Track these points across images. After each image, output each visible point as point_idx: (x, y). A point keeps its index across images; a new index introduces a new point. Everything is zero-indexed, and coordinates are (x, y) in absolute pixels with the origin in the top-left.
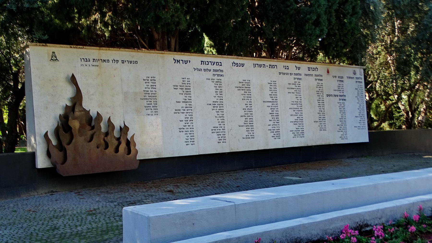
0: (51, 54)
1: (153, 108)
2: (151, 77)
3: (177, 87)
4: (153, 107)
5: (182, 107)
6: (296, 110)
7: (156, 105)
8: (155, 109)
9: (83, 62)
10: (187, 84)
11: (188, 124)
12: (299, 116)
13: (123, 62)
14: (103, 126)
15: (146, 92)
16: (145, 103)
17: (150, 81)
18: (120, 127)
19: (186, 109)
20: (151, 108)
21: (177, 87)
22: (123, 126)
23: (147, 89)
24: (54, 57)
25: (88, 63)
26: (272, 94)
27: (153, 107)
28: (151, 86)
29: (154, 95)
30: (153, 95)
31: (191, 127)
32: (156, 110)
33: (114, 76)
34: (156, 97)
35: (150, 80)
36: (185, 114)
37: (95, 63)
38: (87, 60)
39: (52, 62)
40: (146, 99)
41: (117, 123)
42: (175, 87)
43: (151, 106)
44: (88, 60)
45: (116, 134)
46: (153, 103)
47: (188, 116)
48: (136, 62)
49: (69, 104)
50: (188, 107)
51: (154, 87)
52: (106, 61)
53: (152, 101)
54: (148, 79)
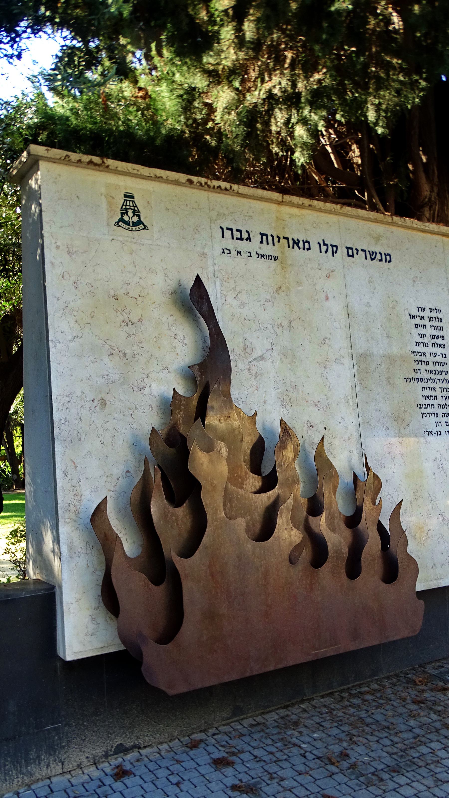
1: (440, 411)
4: (441, 406)
13: (351, 252)
15: (418, 357)
17: (426, 322)
18: (355, 477)
20: (436, 410)
23: (421, 349)
24: (130, 213)
25: (243, 245)
27: (441, 406)
28: (433, 337)
30: (438, 368)
33: (327, 298)
34: (446, 373)
35: (426, 318)
37: (267, 249)
38: (243, 236)
39: (122, 233)
44: (245, 235)
48: (387, 258)
51: (440, 341)
52: (301, 245)
53: (438, 386)
54: (422, 314)
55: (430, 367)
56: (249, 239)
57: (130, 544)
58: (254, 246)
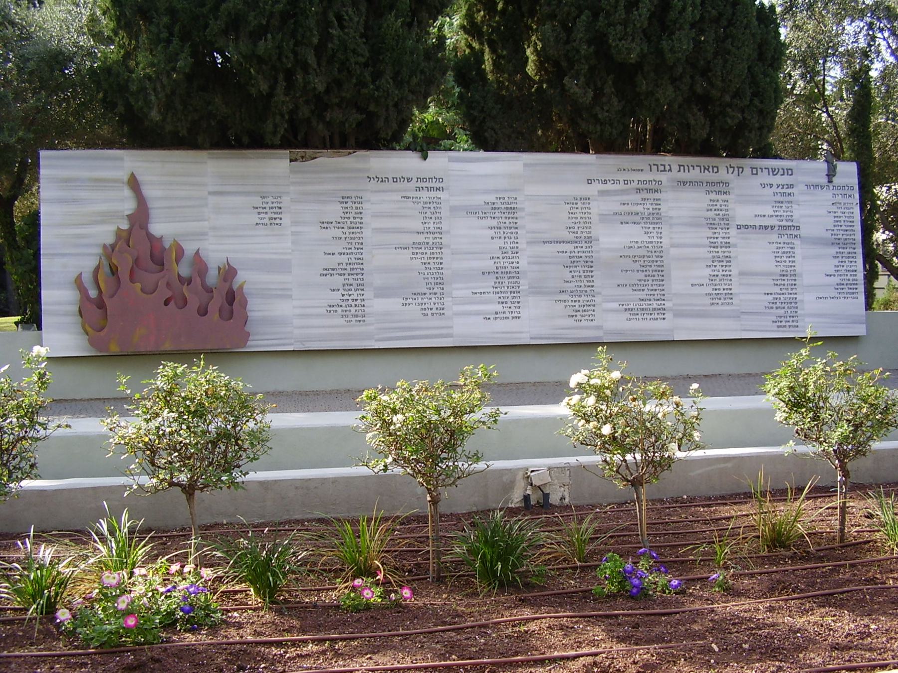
5: (339, 264)
6: (642, 260)
10: (354, 218)
11: (352, 297)
12: (650, 273)
19: (349, 267)
26: (576, 226)
31: (359, 302)
36: (346, 276)
42: (325, 225)
47: (351, 281)
50: (354, 264)
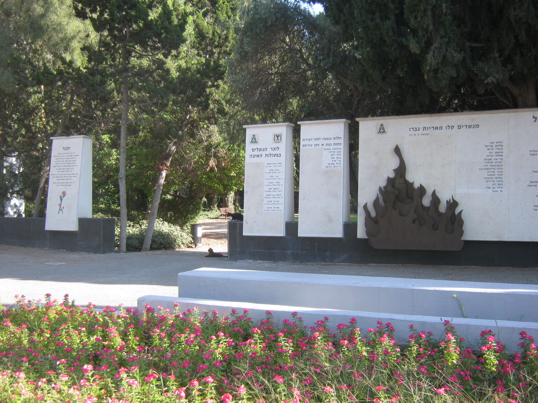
0: (379, 126)
1: (496, 180)
2: (497, 143)
3: (535, 153)
4: (496, 178)
7: (501, 176)
8: (499, 181)
9: (412, 132)
14: (426, 201)
15: (487, 161)
16: (485, 173)
21: (535, 153)
22: (452, 201)
23: (489, 158)
25: (417, 132)
27: (496, 178)
28: (497, 152)
29: (499, 164)
30: (497, 164)
32: (500, 183)
34: (502, 166)
37: (426, 132)
39: (380, 135)
40: (488, 169)
41: (444, 197)
43: (494, 177)
44: (418, 129)
45: (443, 208)
46: (496, 173)
48: (477, 126)
49: (392, 175)
51: (500, 154)
54: (492, 144)
55: (494, 164)
56: (419, 130)
57: (373, 214)
58: (421, 131)
